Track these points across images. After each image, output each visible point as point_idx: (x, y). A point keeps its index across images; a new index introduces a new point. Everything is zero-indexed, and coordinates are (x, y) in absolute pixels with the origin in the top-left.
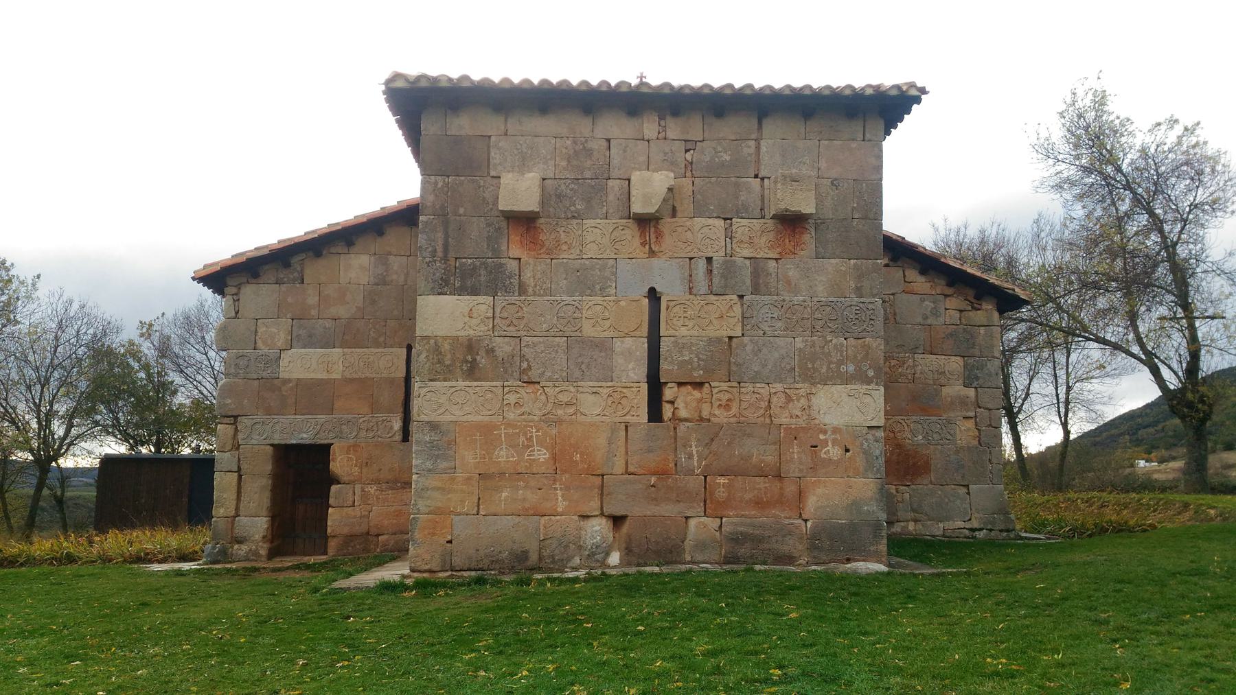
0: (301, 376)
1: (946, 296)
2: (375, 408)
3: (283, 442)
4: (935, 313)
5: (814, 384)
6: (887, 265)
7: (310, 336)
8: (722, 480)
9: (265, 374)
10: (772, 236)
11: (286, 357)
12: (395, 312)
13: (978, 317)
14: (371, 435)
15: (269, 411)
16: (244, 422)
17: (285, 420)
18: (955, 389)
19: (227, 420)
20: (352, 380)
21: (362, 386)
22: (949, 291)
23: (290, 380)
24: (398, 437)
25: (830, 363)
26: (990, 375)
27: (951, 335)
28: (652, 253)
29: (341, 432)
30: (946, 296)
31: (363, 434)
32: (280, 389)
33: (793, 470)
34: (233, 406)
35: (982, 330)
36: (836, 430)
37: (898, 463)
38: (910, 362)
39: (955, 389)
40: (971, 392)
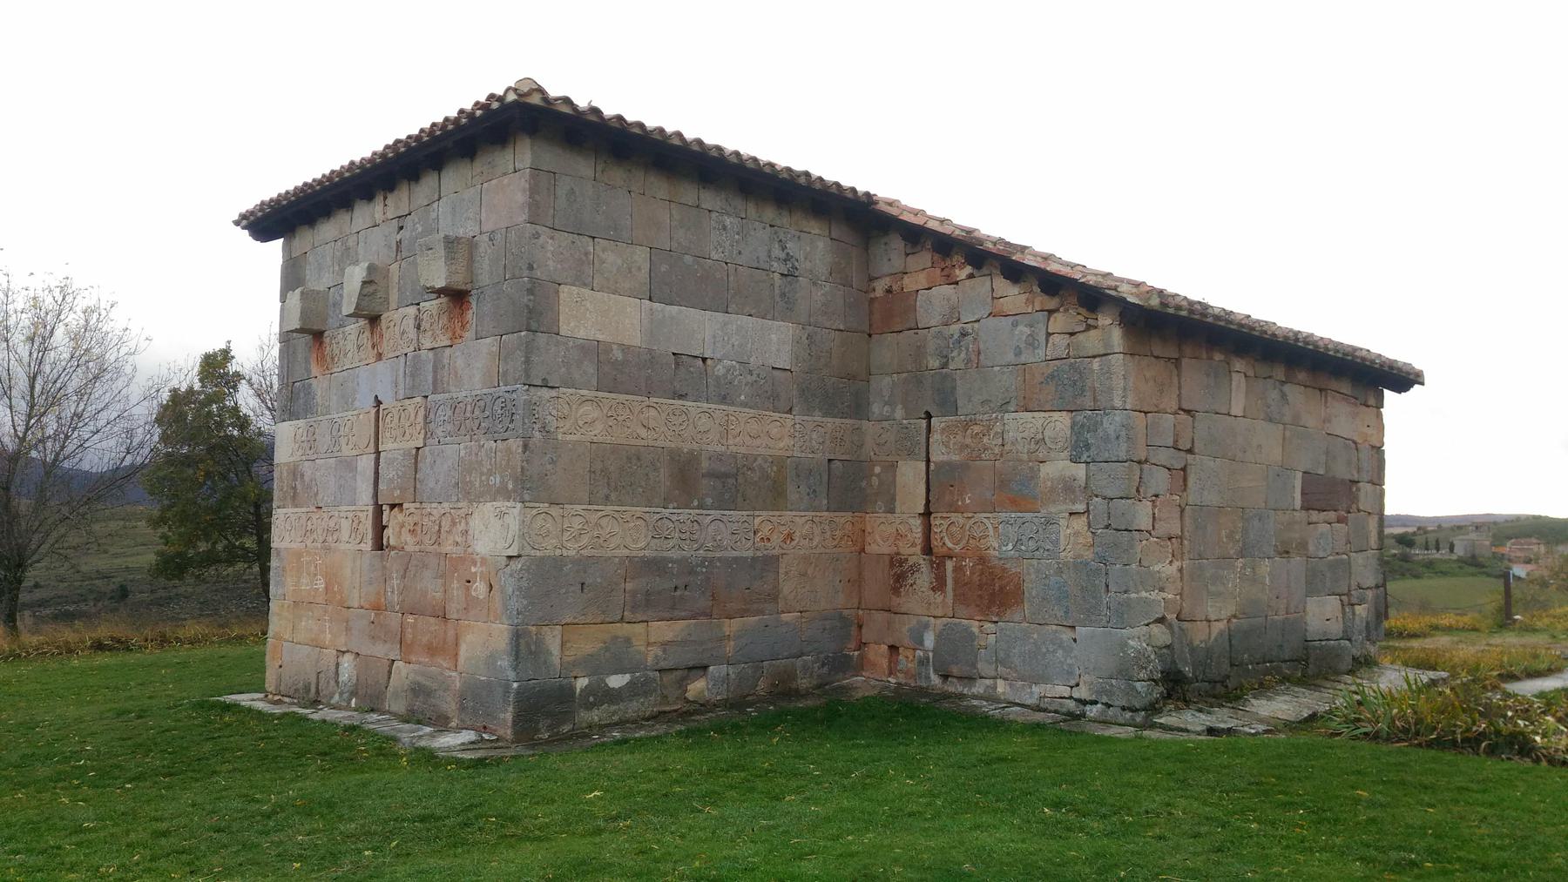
1: (1051, 312)
4: (1032, 343)
5: (470, 501)
6: (971, 276)
8: (410, 619)
10: (444, 320)
13: (1091, 341)
18: (1058, 467)
22: (1052, 303)
25: (482, 474)
26: (1106, 439)
27: (1052, 377)
28: (379, 357)
30: (1051, 312)
33: (453, 611)
35: (1096, 364)
36: (484, 561)
37: (980, 587)
38: (998, 428)
39: (1058, 467)
40: (1080, 471)
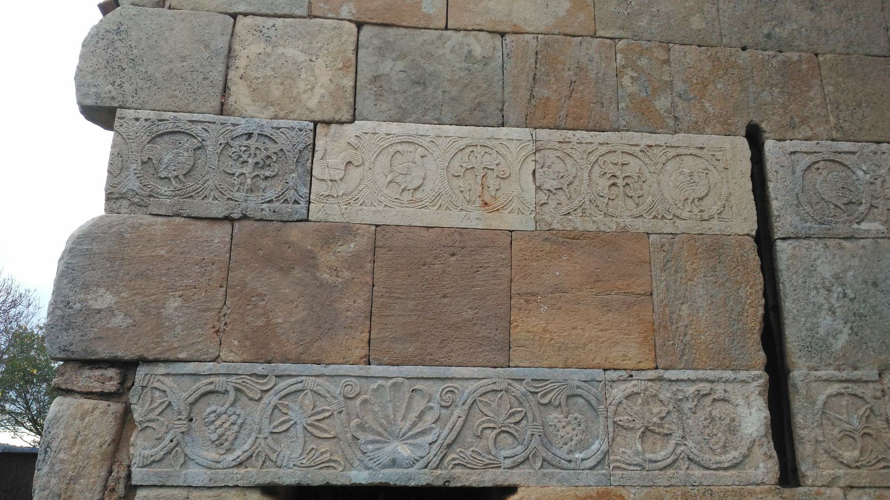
0: (391, 217)
2: (665, 346)
3: (317, 478)
7: (419, 83)
9: (253, 204)
11: (333, 147)
12: (697, 22)
14: (662, 453)
15: (263, 348)
16: (160, 391)
17: (327, 383)
19: (88, 379)
20: (569, 240)
21: (611, 263)
23: (348, 230)
24: (764, 467)
29: (546, 441)
31: (630, 448)
32: (309, 261)
34: (119, 320)
